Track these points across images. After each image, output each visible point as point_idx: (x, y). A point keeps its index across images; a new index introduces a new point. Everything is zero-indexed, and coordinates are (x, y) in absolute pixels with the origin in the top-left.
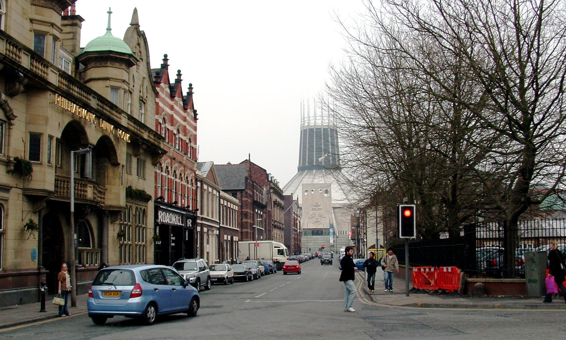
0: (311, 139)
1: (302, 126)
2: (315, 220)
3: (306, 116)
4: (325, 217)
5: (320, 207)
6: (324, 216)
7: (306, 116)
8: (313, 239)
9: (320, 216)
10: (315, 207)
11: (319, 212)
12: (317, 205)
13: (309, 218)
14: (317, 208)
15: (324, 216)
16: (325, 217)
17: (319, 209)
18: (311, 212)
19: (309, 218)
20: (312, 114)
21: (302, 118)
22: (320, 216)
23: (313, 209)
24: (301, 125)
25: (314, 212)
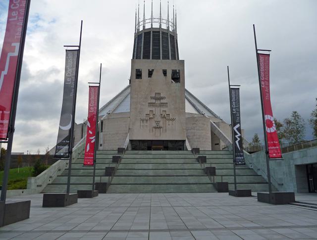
0: (147, 43)
1: (137, 30)
2: (154, 125)
3: (141, 19)
4: (173, 120)
5: (162, 101)
6: (171, 117)
7: (141, 19)
8: (151, 156)
9: (164, 117)
10: (154, 101)
11: (162, 109)
12: (158, 96)
13: (143, 120)
14: (158, 102)
15: (171, 117)
16: (173, 120)
17: (162, 105)
18: (147, 109)
19: (143, 120)
20: (148, 16)
21: (137, 23)
22: (164, 117)
23: (151, 104)
24: (135, 33)
25: (153, 109)
